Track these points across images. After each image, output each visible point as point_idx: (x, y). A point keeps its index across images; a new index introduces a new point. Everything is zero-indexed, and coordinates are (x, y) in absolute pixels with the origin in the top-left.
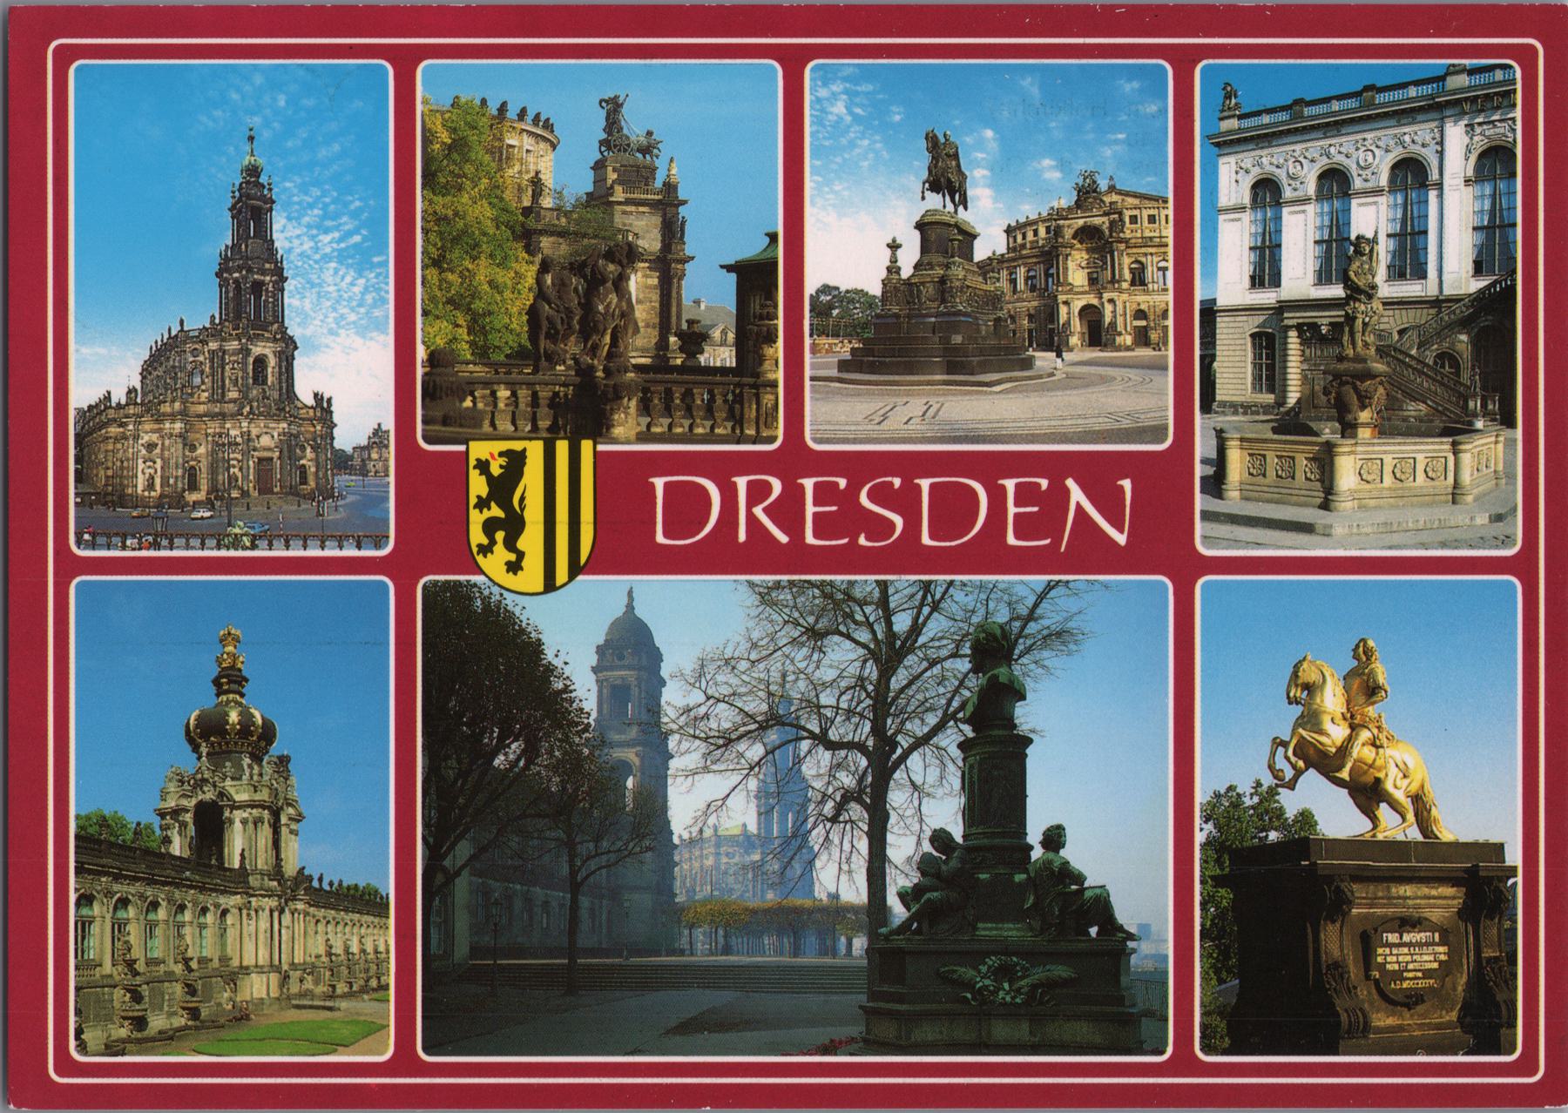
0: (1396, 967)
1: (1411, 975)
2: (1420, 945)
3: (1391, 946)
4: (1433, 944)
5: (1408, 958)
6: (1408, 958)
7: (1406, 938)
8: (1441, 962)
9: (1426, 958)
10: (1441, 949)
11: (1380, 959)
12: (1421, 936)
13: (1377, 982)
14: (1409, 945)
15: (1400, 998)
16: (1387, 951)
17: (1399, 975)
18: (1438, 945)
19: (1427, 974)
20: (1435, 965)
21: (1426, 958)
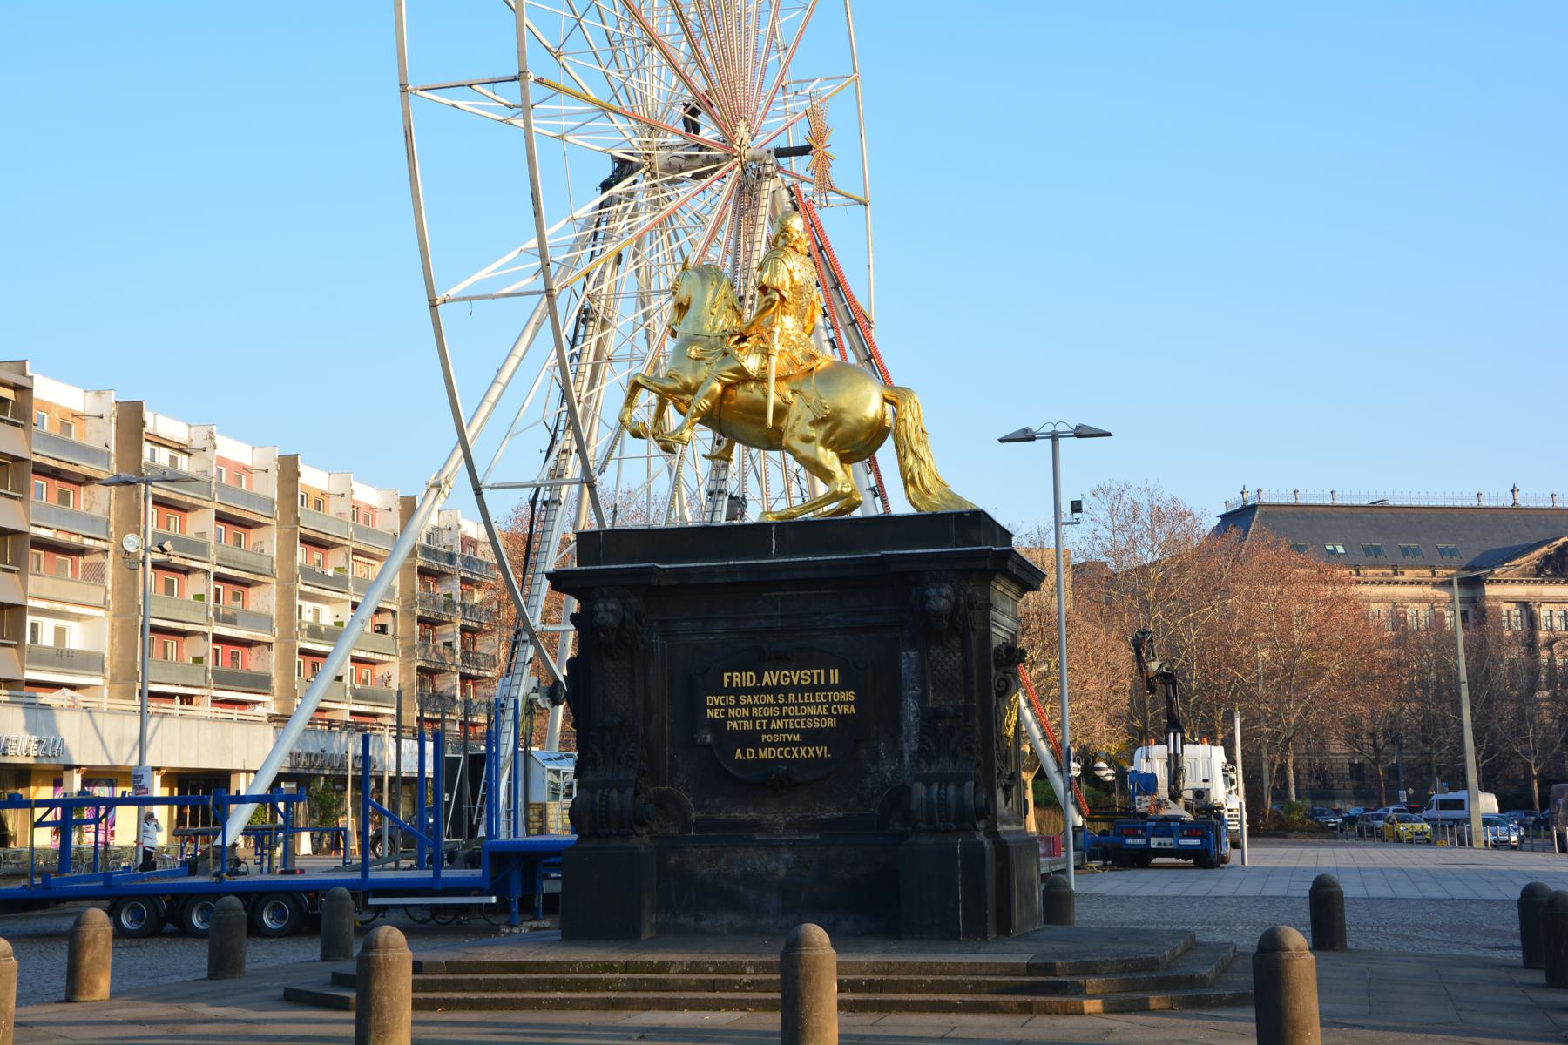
0: (747, 725)
1: (777, 738)
2: (799, 689)
3: (737, 691)
4: (828, 687)
5: (775, 711)
6: (775, 711)
7: (769, 678)
8: (841, 718)
9: (809, 710)
10: (842, 696)
12: (803, 676)
14: (775, 690)
16: (731, 699)
17: (751, 739)
18: (834, 688)
19: (812, 737)
20: (831, 723)
21: (809, 710)
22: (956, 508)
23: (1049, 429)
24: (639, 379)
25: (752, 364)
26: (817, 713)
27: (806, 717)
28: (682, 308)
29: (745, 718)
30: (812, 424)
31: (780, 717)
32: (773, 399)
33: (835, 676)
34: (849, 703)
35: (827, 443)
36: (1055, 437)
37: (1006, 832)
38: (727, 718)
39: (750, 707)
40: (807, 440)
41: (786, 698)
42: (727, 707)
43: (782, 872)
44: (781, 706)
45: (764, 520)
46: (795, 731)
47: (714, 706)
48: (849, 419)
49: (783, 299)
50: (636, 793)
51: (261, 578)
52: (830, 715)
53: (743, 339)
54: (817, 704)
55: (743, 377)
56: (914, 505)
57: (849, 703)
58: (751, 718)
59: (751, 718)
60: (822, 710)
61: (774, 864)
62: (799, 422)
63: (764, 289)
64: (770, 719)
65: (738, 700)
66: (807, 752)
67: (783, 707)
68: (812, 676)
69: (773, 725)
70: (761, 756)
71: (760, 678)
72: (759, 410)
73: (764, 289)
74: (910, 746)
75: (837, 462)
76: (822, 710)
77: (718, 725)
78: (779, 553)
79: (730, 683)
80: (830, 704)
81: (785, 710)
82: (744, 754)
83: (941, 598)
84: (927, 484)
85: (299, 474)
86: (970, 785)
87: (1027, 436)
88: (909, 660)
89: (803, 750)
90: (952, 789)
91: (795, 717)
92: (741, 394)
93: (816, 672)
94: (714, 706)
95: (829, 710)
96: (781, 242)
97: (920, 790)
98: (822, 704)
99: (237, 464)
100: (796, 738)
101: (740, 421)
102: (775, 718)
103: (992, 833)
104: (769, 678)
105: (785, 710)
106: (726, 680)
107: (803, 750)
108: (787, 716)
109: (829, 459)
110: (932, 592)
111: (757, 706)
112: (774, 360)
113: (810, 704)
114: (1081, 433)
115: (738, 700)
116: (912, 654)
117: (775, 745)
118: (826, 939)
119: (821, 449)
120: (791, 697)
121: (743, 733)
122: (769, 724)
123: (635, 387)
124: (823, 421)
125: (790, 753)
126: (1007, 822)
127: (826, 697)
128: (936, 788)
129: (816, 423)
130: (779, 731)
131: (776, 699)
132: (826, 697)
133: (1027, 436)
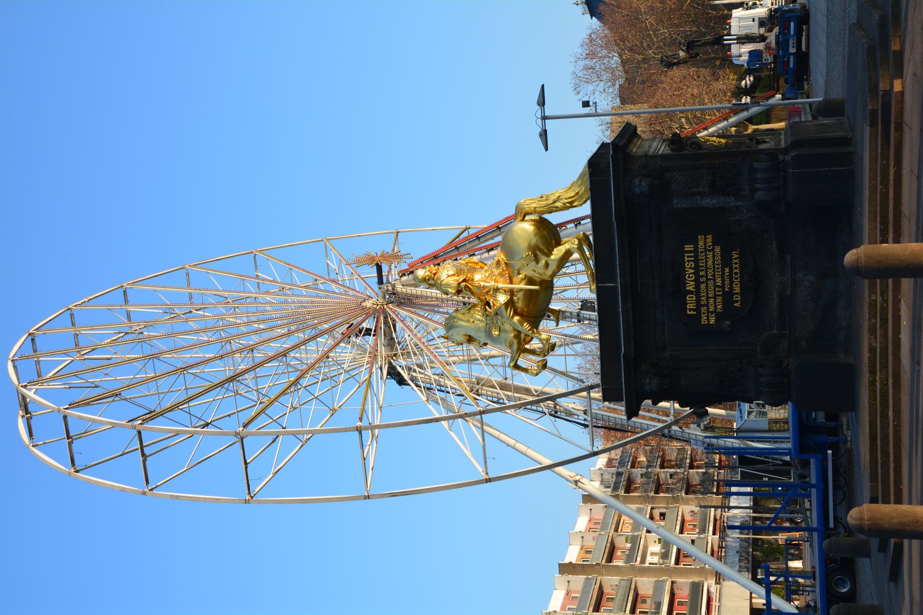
0: (719, 299)
2: (697, 269)
3: (699, 305)
4: (696, 251)
5: (711, 283)
6: (711, 283)
7: (690, 286)
8: (715, 243)
9: (710, 262)
10: (701, 243)
14: (697, 282)
16: (703, 309)
17: (728, 297)
18: (696, 248)
19: (726, 261)
20: (717, 249)
21: (710, 262)
22: (587, 177)
23: (539, 122)
24: (512, 365)
25: (502, 298)
26: (712, 258)
27: (714, 264)
28: (470, 340)
29: (715, 301)
30: (537, 262)
31: (714, 280)
32: (522, 286)
33: (689, 247)
34: (705, 239)
35: (549, 254)
36: (544, 118)
37: (785, 142)
38: (715, 311)
39: (708, 298)
40: (547, 265)
41: (703, 276)
42: (708, 312)
43: (811, 278)
44: (708, 279)
45: (595, 290)
46: (723, 271)
47: (708, 320)
48: (534, 241)
49: (464, 281)
50: (762, 366)
51: (633, 587)
52: (713, 250)
53: (488, 304)
54: (706, 258)
55: (510, 303)
56: (585, 202)
57: (705, 239)
60: (710, 255)
61: (806, 283)
62: (537, 270)
63: (459, 292)
64: (715, 286)
65: (704, 305)
66: (736, 263)
67: (708, 278)
68: (689, 261)
69: (719, 284)
70: (738, 291)
71: (691, 292)
72: (529, 294)
73: (459, 292)
74: (732, 202)
75: (560, 247)
76: (710, 255)
77: (719, 317)
78: (615, 282)
79: (693, 310)
80: (706, 250)
81: (710, 277)
82: (737, 301)
83: (641, 185)
84: (572, 194)
85: (571, 563)
86: (756, 165)
87: (544, 135)
88: (679, 203)
89: (735, 266)
90: (758, 176)
91: (714, 271)
92: (520, 305)
93: (686, 259)
94: (708, 320)
95: (710, 251)
96: (431, 282)
97: (759, 195)
98: (706, 255)
99: (564, 599)
100: (727, 270)
101: (536, 305)
102: (715, 282)
103: (786, 151)
104: (690, 286)
105: (710, 277)
106: (692, 312)
107: (735, 266)
108: (714, 275)
109: (558, 252)
110: (637, 190)
111: (707, 294)
112: (500, 285)
113: (706, 262)
114: (542, 102)
115: (704, 305)
116: (675, 201)
117: (731, 282)
118: (854, 251)
119: (552, 257)
120: (702, 273)
121: (724, 302)
122: (719, 287)
123: (516, 367)
124: (536, 256)
125: (736, 274)
126: (780, 141)
127: (702, 252)
128: (758, 186)
129: (537, 260)
130: (723, 280)
131: (703, 283)
132: (702, 252)
133: (544, 135)
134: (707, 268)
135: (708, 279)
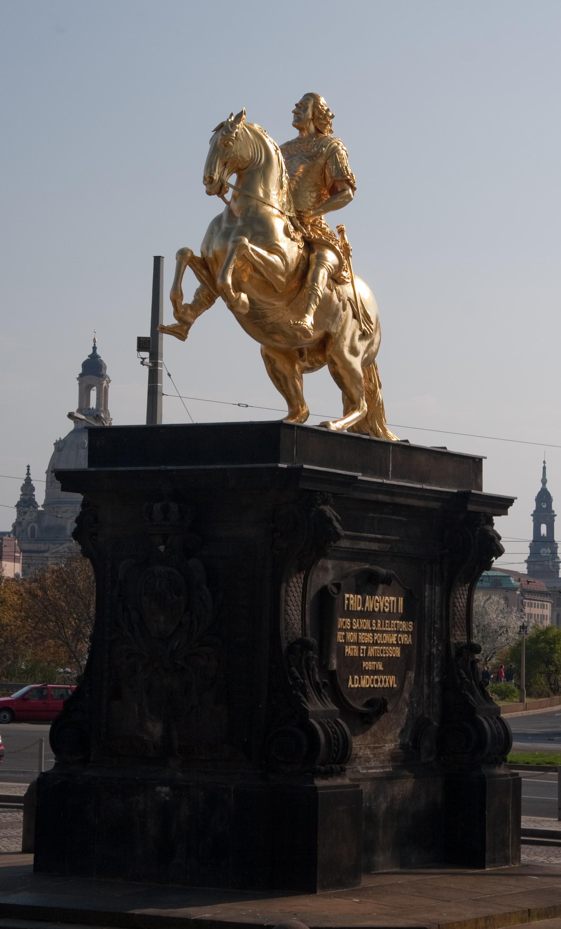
8: (403, 647)
11: (340, 637)
13: (332, 675)
15: (358, 705)
17: (355, 666)
19: (390, 665)
20: (397, 652)
34: (407, 633)
39: (358, 631)
41: (376, 624)
52: (397, 645)
57: (407, 633)
58: (358, 644)
59: (358, 644)
70: (365, 682)
91: (381, 645)
93: (392, 598)
98: (394, 632)
105: (377, 636)
111: (362, 631)
129: (364, 335)
134: (383, 632)
135: (373, 632)
